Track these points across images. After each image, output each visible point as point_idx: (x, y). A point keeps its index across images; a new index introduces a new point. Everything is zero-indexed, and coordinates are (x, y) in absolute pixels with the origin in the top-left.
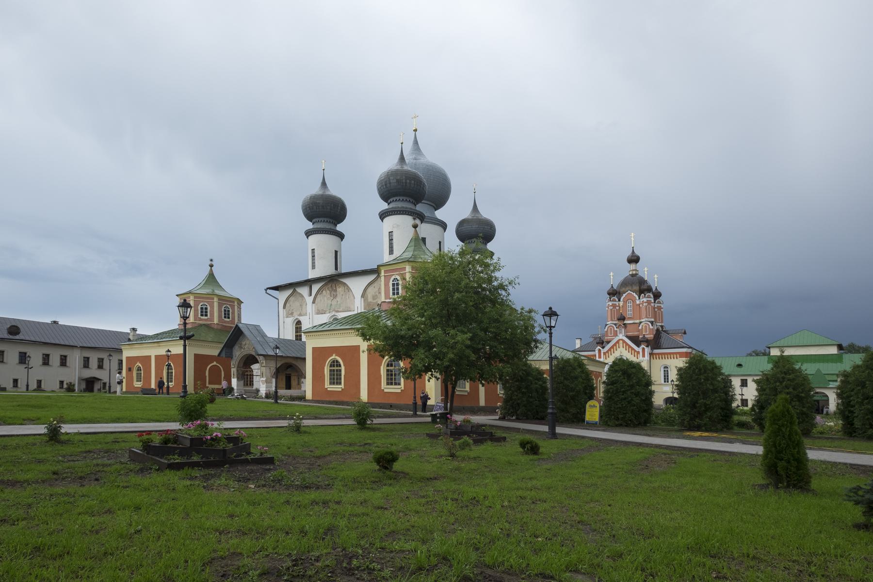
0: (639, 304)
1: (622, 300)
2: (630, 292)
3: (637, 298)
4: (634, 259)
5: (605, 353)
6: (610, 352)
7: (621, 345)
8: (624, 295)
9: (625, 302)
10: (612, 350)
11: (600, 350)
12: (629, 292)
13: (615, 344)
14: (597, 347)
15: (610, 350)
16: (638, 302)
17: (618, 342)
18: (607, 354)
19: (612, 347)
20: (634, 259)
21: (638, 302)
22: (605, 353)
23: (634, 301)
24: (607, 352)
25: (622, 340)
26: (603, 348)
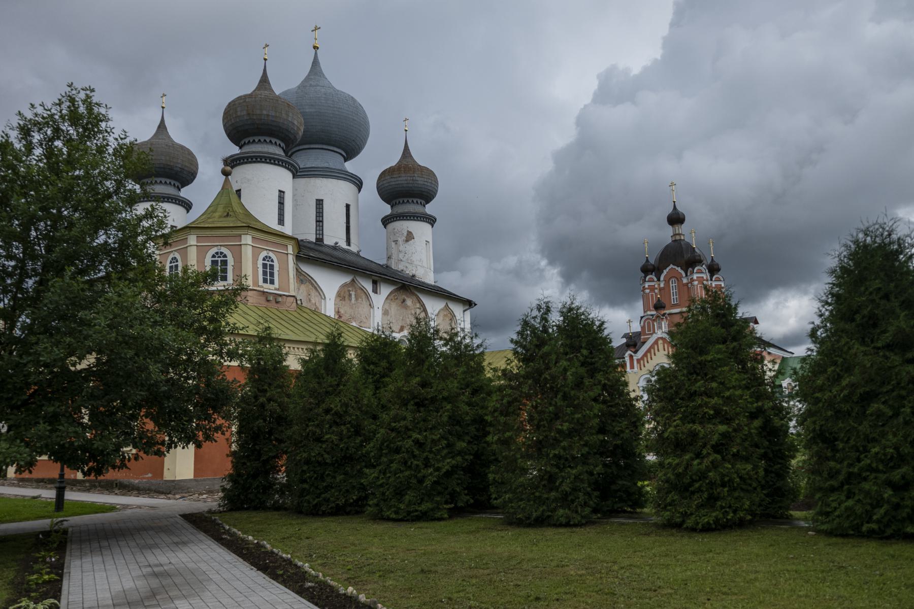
0: (688, 284)
1: (662, 278)
2: (674, 267)
3: (684, 275)
4: (676, 219)
5: (638, 361)
6: (645, 359)
7: (661, 347)
8: (665, 272)
9: (667, 282)
10: (649, 355)
11: (631, 357)
12: (671, 266)
13: (652, 347)
14: (627, 351)
15: (645, 355)
16: (685, 281)
17: (656, 342)
18: (642, 362)
19: (649, 351)
20: (676, 219)
21: (685, 281)
22: (638, 361)
23: (679, 279)
24: (642, 358)
25: (662, 338)
26: (635, 352)
